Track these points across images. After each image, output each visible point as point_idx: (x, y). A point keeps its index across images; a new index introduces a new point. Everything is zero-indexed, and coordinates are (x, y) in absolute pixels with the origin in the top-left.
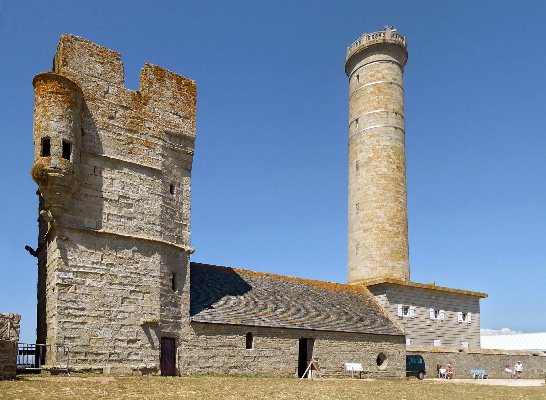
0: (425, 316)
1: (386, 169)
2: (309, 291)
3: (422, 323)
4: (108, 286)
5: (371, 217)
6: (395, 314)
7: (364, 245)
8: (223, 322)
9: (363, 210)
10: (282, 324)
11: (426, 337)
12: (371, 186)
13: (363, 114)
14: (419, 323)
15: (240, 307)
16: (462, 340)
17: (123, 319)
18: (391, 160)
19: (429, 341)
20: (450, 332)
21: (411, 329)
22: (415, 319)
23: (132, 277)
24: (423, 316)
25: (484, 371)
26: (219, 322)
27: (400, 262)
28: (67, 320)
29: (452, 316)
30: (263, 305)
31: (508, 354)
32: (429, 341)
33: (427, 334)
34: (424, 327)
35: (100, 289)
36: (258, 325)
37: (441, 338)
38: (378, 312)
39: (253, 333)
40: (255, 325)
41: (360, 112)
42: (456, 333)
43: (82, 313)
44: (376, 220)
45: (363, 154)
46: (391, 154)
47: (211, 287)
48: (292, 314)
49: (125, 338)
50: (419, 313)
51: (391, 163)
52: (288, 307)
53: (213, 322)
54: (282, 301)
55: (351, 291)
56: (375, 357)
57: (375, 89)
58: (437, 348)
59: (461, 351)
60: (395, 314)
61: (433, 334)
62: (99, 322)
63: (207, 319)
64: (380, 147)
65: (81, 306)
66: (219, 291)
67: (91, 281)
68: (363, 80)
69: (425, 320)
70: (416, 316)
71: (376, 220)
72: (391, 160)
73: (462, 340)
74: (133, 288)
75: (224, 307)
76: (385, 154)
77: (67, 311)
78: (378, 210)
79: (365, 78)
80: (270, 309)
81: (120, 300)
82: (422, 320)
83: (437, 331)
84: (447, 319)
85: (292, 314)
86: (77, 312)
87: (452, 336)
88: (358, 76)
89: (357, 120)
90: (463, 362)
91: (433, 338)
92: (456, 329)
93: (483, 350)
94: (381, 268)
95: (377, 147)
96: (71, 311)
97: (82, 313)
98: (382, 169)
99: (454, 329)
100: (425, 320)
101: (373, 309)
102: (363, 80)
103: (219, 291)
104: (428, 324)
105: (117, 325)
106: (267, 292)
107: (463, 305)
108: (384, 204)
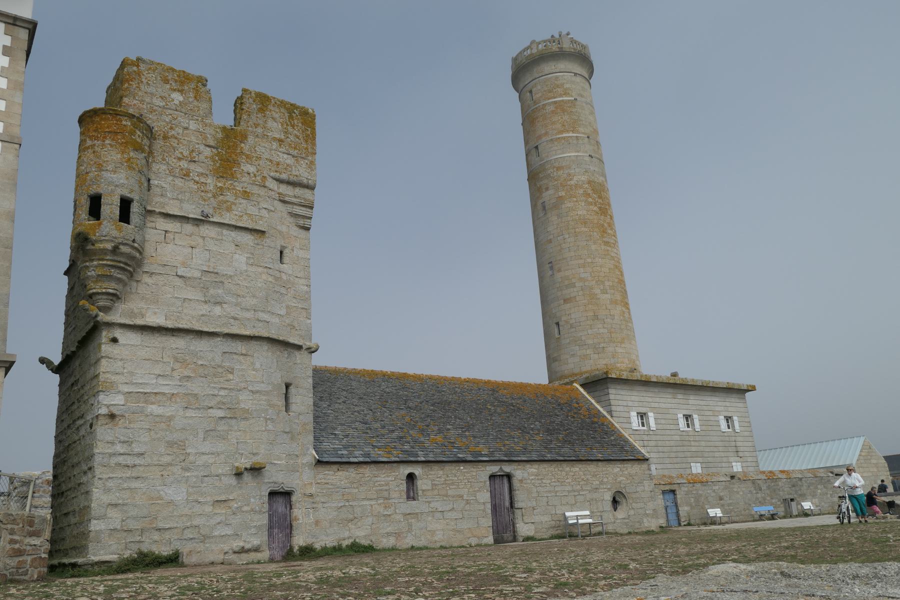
0: (672, 427)
1: (585, 212)
2: (495, 399)
3: (669, 438)
4: (181, 413)
5: (573, 281)
6: (627, 426)
7: (567, 322)
8: (368, 460)
9: (559, 271)
10: (460, 456)
11: (679, 460)
12: (567, 236)
13: (544, 139)
14: (665, 438)
15: (393, 431)
16: (731, 459)
17: (206, 466)
18: (590, 200)
19: (684, 465)
20: (712, 449)
21: (655, 449)
22: (659, 432)
23: (222, 396)
24: (668, 427)
25: (771, 508)
26: (361, 459)
27: (623, 345)
28: (111, 475)
29: (711, 423)
30: (428, 426)
31: (800, 476)
32: (684, 465)
33: (680, 455)
34: (672, 443)
35: (171, 418)
36: (423, 459)
37: (700, 460)
38: (603, 424)
39: (417, 473)
40: (419, 459)
41: (540, 137)
42: (721, 449)
43: (138, 461)
44: (581, 284)
45: (551, 192)
46: (590, 191)
47: (344, 402)
48: (475, 437)
49: (209, 499)
50: (663, 421)
51: (591, 204)
52: (468, 427)
53: (352, 460)
54: (455, 417)
55: (558, 394)
56: (608, 497)
57: (556, 108)
58: (696, 475)
59: (732, 477)
60: (627, 426)
61: (689, 454)
62: (165, 473)
63: (342, 456)
64: (572, 182)
65: (136, 450)
66: (357, 409)
67: (153, 407)
68: (538, 96)
69: (673, 432)
70: (660, 427)
71: (581, 284)
72: (590, 200)
73: (731, 459)
74: (221, 413)
75: (367, 433)
76: (581, 191)
77: (114, 461)
78: (582, 270)
79: (540, 94)
80: (440, 431)
81: (201, 435)
82: (668, 432)
83: (693, 449)
84: (704, 428)
85: (475, 437)
86: (130, 461)
87: (717, 454)
88: (531, 92)
89: (537, 147)
90: (738, 496)
91: (690, 460)
92: (720, 444)
93: (764, 472)
94: (596, 356)
95: (569, 183)
96: (121, 459)
97: (138, 461)
98: (580, 213)
99: (717, 444)
100: (673, 432)
101: (596, 420)
102: (538, 96)
103: (357, 409)
104: (677, 438)
105: (196, 477)
106: (432, 405)
107: (724, 404)
108: (589, 260)
